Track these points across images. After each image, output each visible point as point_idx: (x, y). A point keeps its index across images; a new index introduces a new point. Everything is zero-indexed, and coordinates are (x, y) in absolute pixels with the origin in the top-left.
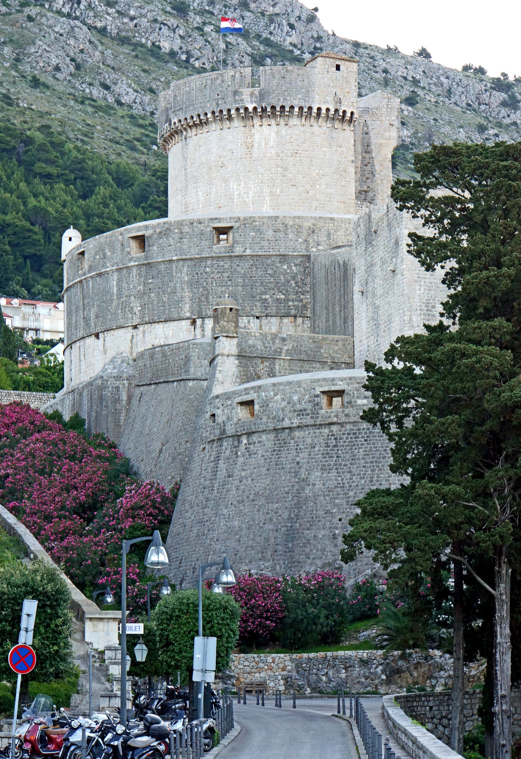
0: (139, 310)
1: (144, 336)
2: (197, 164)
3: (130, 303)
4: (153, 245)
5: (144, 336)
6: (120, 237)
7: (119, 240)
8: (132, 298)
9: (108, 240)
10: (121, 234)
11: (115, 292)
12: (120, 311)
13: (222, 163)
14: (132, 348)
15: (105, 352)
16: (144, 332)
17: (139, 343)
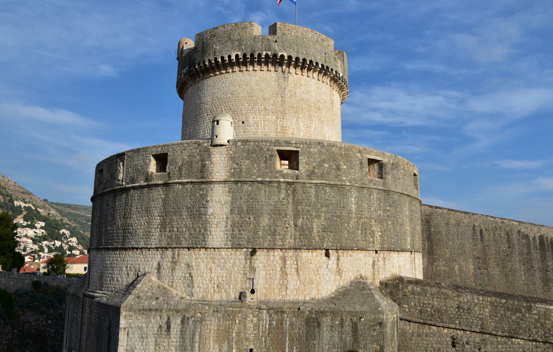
0: (380, 236)
1: (384, 263)
2: (298, 99)
3: (371, 226)
4: (389, 174)
5: (384, 263)
6: (358, 155)
7: (356, 157)
8: (373, 221)
9: (343, 153)
10: (360, 152)
11: (354, 210)
12: (360, 232)
13: (319, 107)
14: (374, 274)
15: (339, 272)
16: (384, 259)
17: (381, 270)
